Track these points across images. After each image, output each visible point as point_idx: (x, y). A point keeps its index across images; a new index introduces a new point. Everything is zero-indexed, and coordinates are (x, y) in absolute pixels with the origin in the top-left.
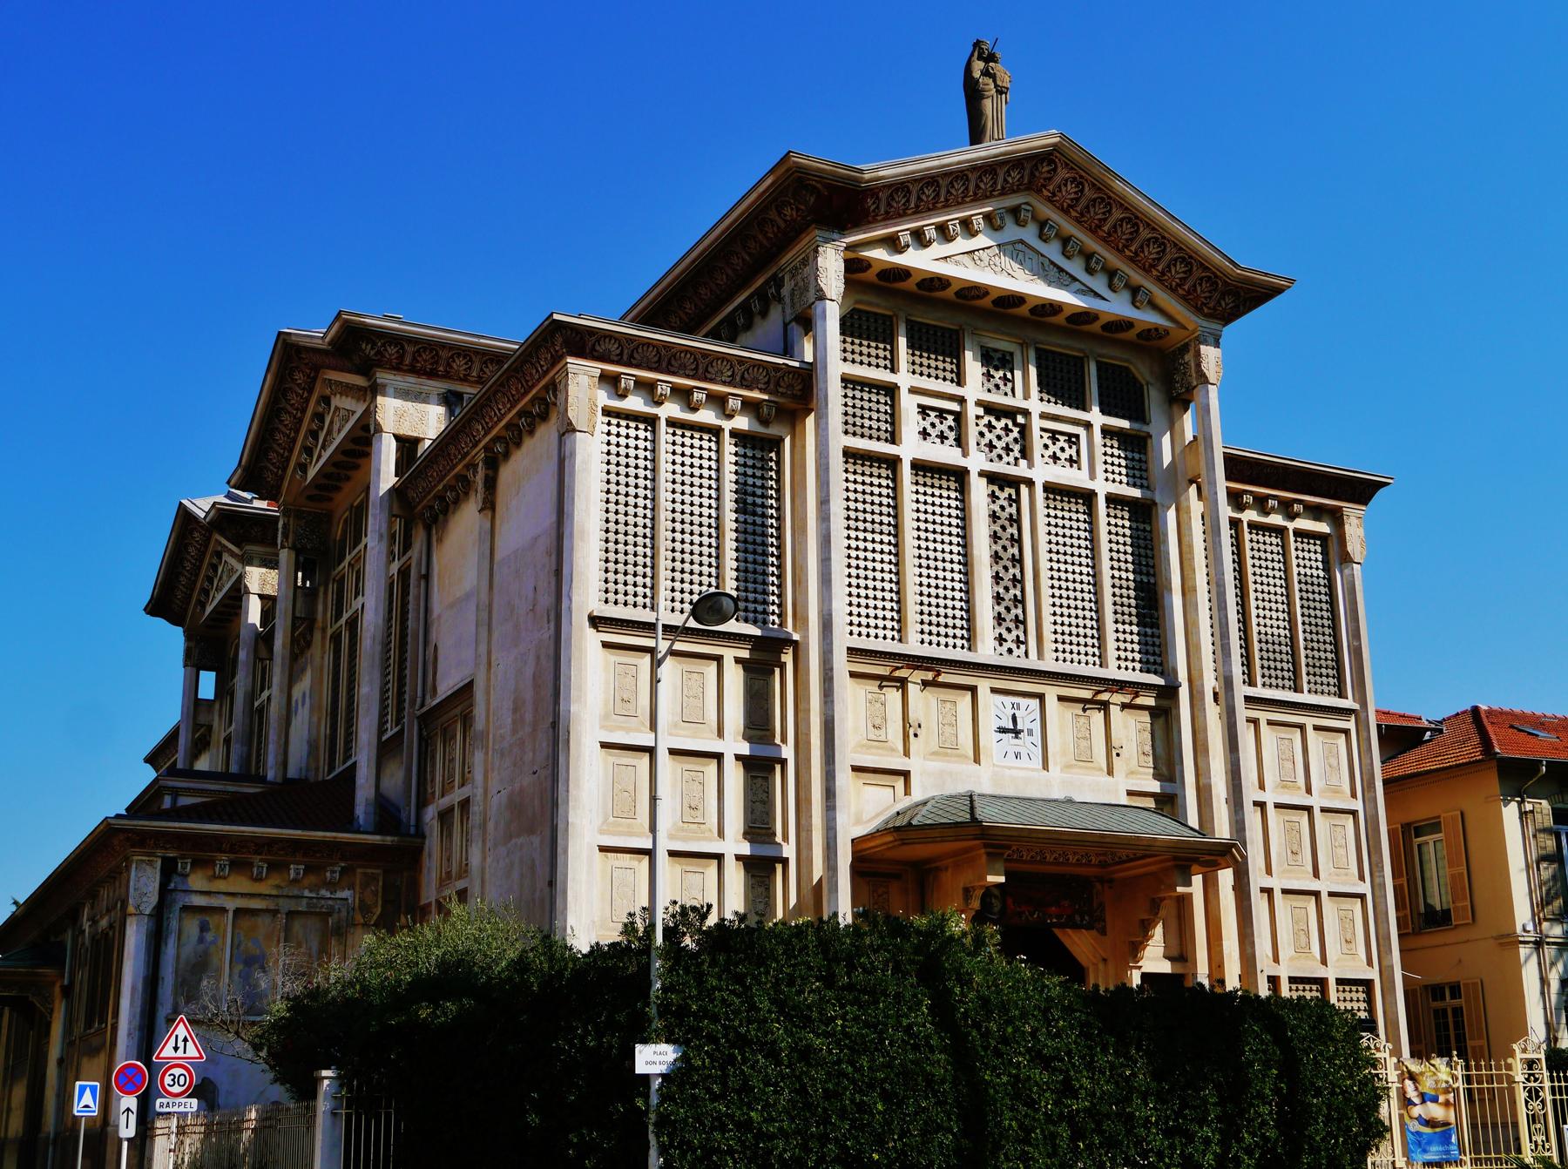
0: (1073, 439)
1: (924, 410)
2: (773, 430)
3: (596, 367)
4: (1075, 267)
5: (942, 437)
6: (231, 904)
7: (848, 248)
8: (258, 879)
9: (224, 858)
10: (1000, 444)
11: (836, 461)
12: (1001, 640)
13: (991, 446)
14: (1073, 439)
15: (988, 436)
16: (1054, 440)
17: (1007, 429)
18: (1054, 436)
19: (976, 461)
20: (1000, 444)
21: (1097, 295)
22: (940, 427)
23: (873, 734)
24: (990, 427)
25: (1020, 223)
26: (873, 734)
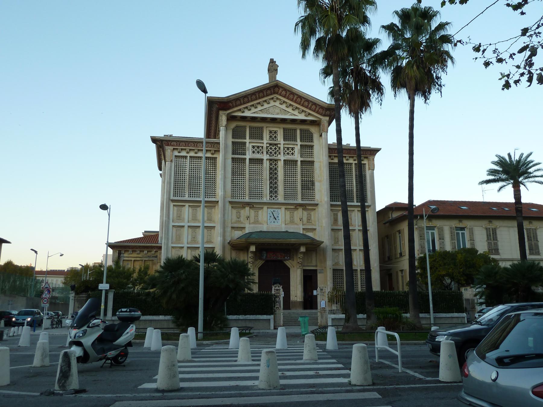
0: (293, 149)
1: (253, 147)
2: (214, 156)
3: (172, 148)
4: (290, 110)
5: (258, 152)
6: (133, 259)
7: (228, 114)
8: (138, 254)
9: (130, 250)
10: (273, 152)
11: (229, 161)
12: (271, 196)
13: (271, 153)
14: (293, 149)
15: (270, 151)
16: (288, 149)
17: (275, 149)
18: (288, 149)
19: (265, 157)
20: (273, 152)
21: (295, 115)
22: (258, 150)
23: (238, 219)
24: (271, 148)
25: (275, 101)
26: (238, 219)
